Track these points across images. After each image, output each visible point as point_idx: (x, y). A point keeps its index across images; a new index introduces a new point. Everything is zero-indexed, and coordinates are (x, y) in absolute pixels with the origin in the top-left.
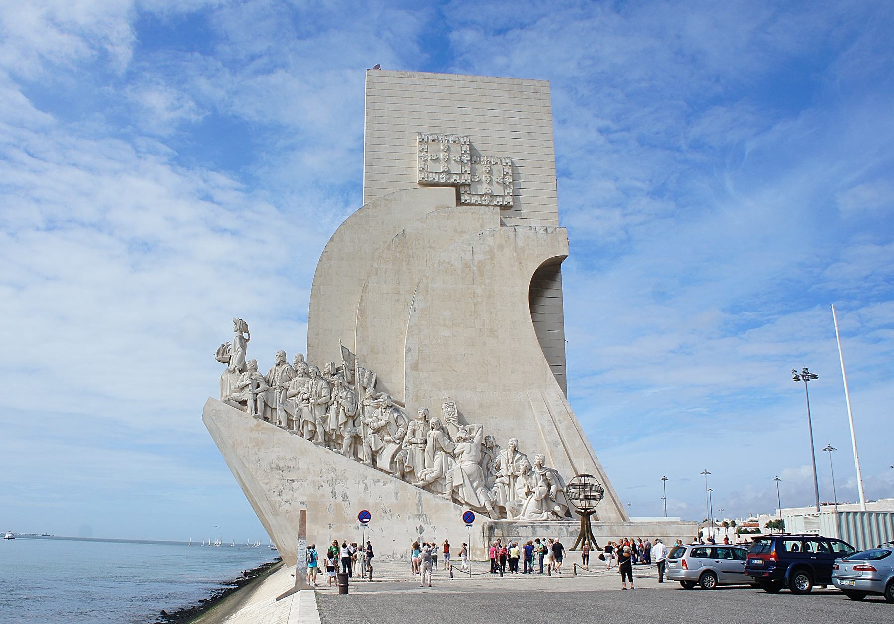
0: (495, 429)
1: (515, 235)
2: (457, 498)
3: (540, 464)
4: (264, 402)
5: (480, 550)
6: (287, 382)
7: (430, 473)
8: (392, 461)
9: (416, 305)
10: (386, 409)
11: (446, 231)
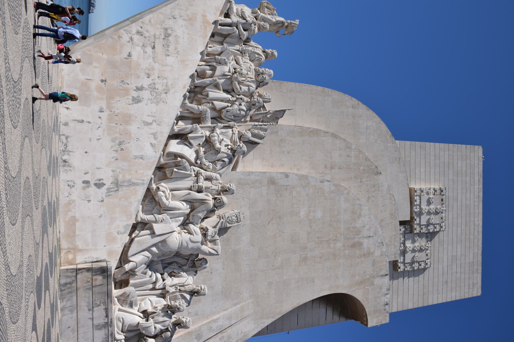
0: (213, 269)
1: (382, 276)
2: (138, 228)
4: (229, 34)
5: (74, 259)
6: (248, 58)
7: (166, 197)
8: (176, 156)
9: (326, 183)
10: (232, 149)
11: (381, 211)
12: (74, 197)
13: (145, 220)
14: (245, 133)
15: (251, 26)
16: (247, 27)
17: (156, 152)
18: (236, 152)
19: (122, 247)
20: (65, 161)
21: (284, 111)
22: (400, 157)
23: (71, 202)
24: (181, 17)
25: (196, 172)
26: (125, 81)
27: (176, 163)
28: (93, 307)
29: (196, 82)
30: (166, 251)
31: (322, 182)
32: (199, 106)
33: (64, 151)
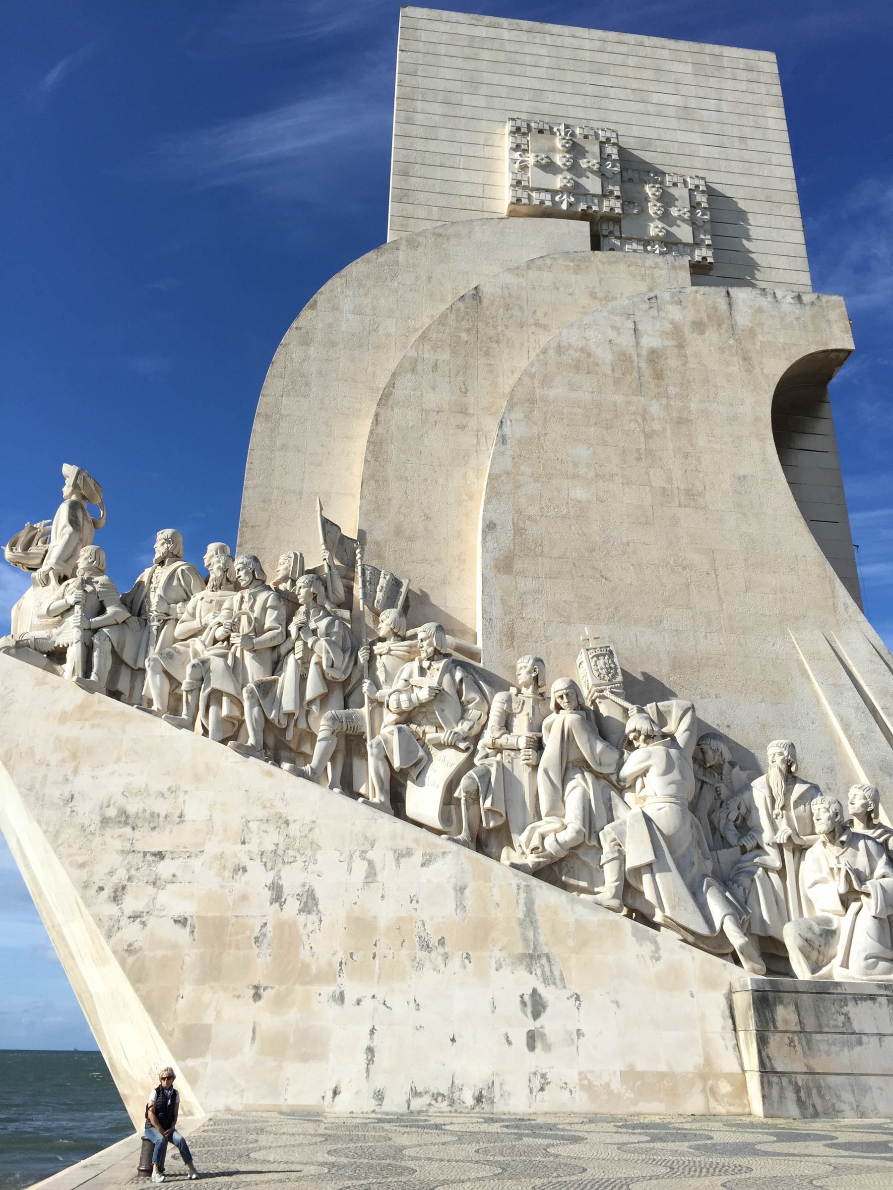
1: (730, 305)
2: (638, 906)
3: (869, 813)
4: (113, 652)
5: (729, 1077)
6: (180, 604)
7: (556, 832)
9: (507, 430)
10: (430, 659)
11: (571, 294)
12: (571, 1076)
13: (617, 887)
14: (388, 625)
15: (91, 592)
16: (93, 603)
17: (444, 853)
18: (438, 648)
19: (691, 951)
20: (479, 1099)
21: (325, 522)
22: (434, 234)
23: (586, 1082)
24: (67, 780)
25: (489, 751)
26: (256, 933)
27: (471, 801)
28: (853, 1033)
29: (251, 741)
30: (690, 837)
31: (503, 439)
32: (318, 739)
33: (452, 1102)
